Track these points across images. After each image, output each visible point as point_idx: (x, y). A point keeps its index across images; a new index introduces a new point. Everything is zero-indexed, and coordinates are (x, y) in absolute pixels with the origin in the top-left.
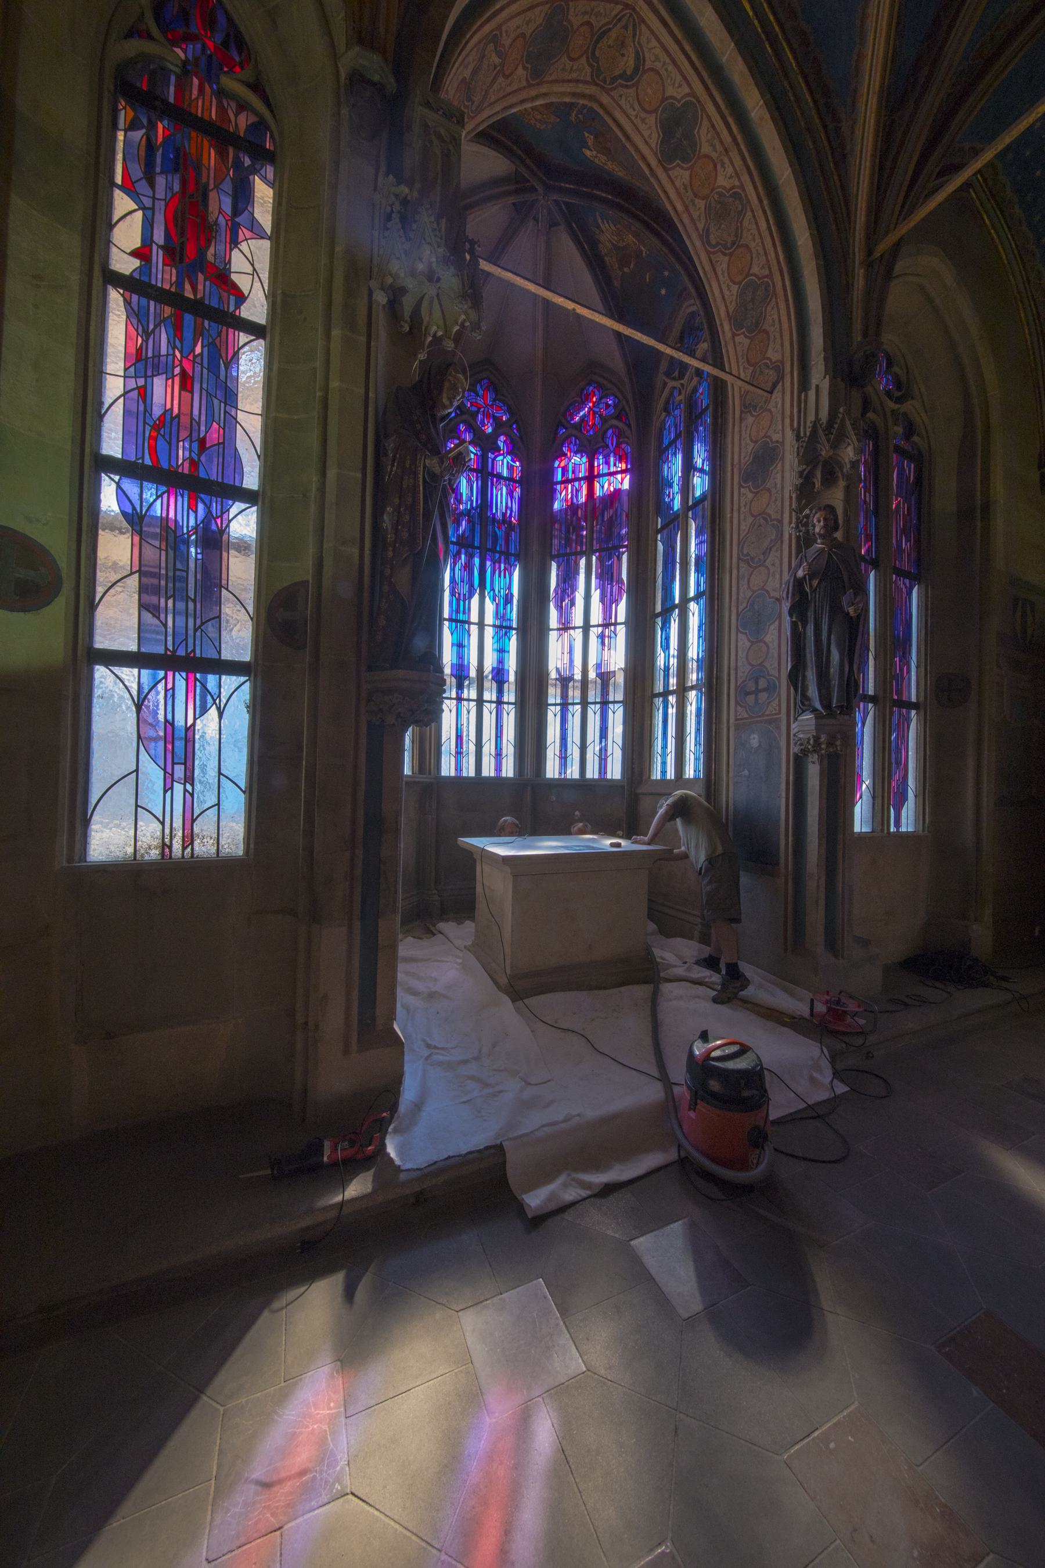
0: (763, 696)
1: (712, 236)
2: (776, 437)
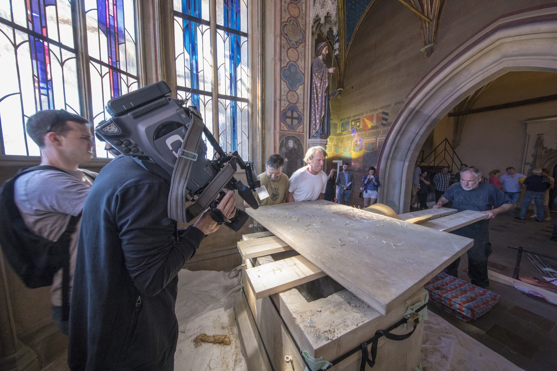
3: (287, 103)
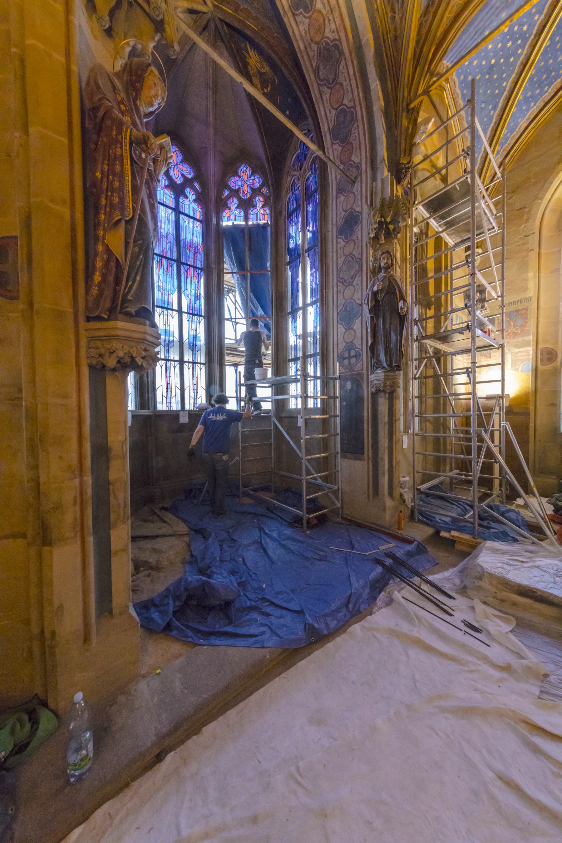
0: (353, 360)
1: (321, 73)
2: (358, 209)
3: (344, 344)
